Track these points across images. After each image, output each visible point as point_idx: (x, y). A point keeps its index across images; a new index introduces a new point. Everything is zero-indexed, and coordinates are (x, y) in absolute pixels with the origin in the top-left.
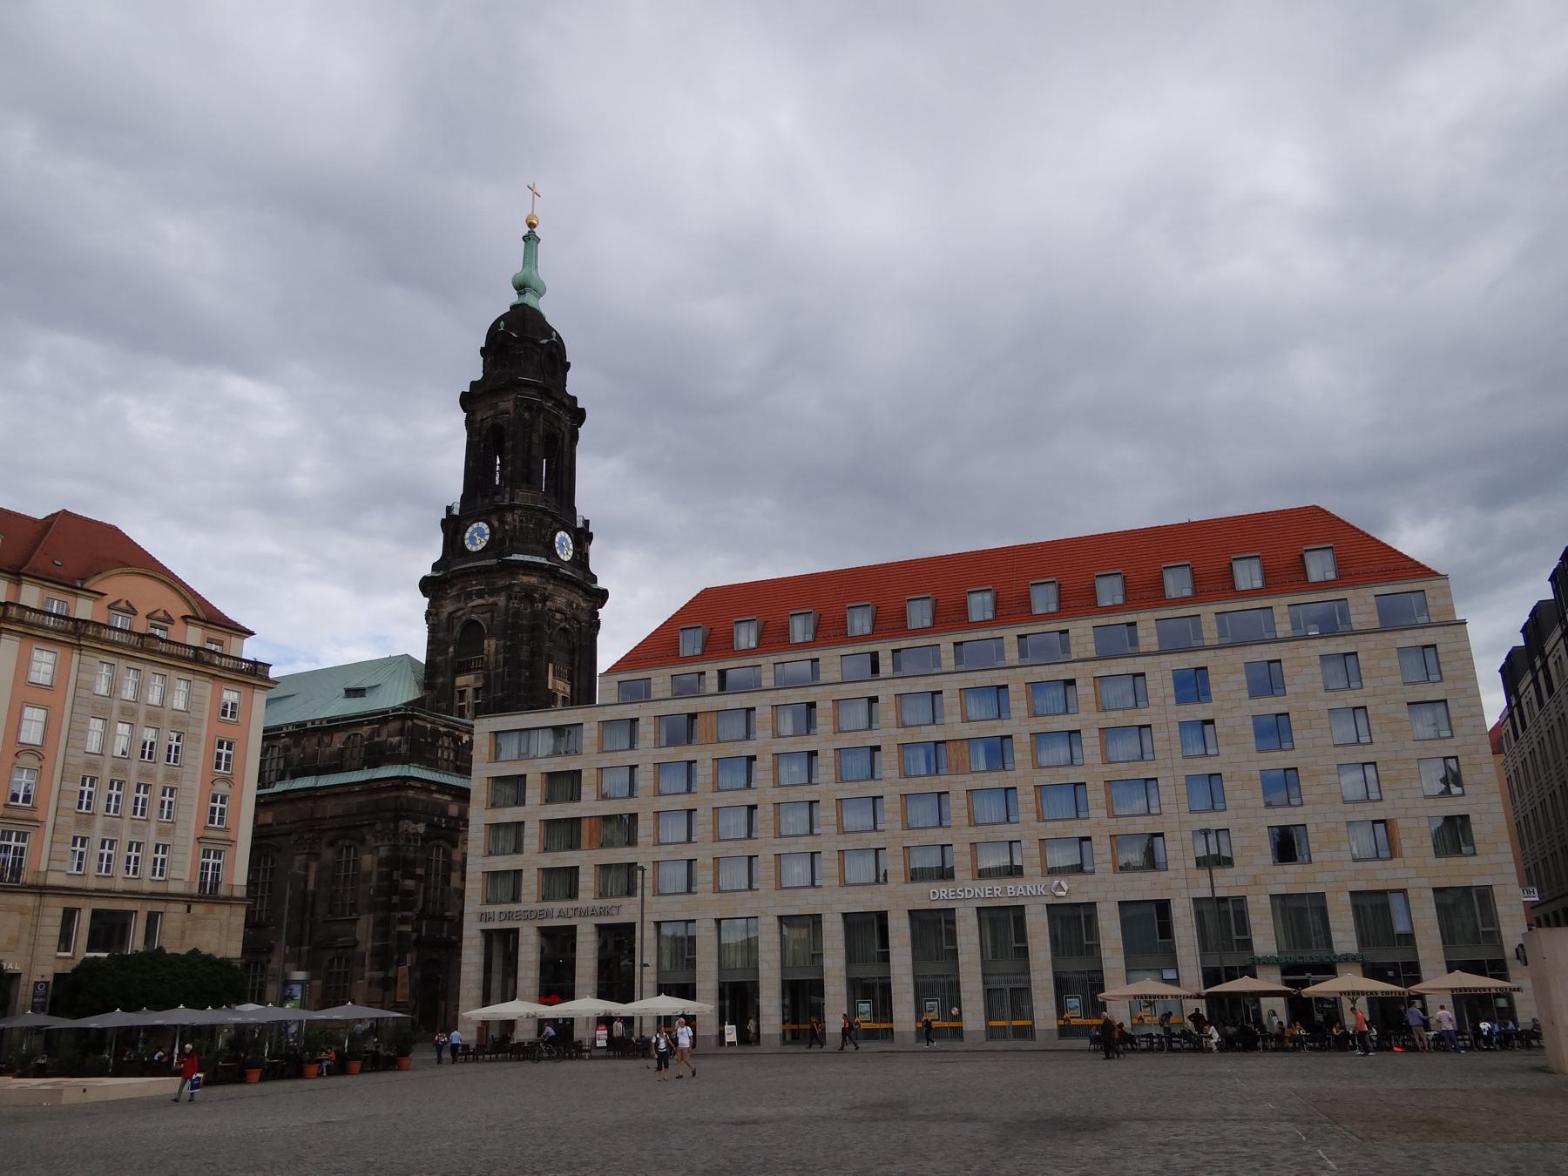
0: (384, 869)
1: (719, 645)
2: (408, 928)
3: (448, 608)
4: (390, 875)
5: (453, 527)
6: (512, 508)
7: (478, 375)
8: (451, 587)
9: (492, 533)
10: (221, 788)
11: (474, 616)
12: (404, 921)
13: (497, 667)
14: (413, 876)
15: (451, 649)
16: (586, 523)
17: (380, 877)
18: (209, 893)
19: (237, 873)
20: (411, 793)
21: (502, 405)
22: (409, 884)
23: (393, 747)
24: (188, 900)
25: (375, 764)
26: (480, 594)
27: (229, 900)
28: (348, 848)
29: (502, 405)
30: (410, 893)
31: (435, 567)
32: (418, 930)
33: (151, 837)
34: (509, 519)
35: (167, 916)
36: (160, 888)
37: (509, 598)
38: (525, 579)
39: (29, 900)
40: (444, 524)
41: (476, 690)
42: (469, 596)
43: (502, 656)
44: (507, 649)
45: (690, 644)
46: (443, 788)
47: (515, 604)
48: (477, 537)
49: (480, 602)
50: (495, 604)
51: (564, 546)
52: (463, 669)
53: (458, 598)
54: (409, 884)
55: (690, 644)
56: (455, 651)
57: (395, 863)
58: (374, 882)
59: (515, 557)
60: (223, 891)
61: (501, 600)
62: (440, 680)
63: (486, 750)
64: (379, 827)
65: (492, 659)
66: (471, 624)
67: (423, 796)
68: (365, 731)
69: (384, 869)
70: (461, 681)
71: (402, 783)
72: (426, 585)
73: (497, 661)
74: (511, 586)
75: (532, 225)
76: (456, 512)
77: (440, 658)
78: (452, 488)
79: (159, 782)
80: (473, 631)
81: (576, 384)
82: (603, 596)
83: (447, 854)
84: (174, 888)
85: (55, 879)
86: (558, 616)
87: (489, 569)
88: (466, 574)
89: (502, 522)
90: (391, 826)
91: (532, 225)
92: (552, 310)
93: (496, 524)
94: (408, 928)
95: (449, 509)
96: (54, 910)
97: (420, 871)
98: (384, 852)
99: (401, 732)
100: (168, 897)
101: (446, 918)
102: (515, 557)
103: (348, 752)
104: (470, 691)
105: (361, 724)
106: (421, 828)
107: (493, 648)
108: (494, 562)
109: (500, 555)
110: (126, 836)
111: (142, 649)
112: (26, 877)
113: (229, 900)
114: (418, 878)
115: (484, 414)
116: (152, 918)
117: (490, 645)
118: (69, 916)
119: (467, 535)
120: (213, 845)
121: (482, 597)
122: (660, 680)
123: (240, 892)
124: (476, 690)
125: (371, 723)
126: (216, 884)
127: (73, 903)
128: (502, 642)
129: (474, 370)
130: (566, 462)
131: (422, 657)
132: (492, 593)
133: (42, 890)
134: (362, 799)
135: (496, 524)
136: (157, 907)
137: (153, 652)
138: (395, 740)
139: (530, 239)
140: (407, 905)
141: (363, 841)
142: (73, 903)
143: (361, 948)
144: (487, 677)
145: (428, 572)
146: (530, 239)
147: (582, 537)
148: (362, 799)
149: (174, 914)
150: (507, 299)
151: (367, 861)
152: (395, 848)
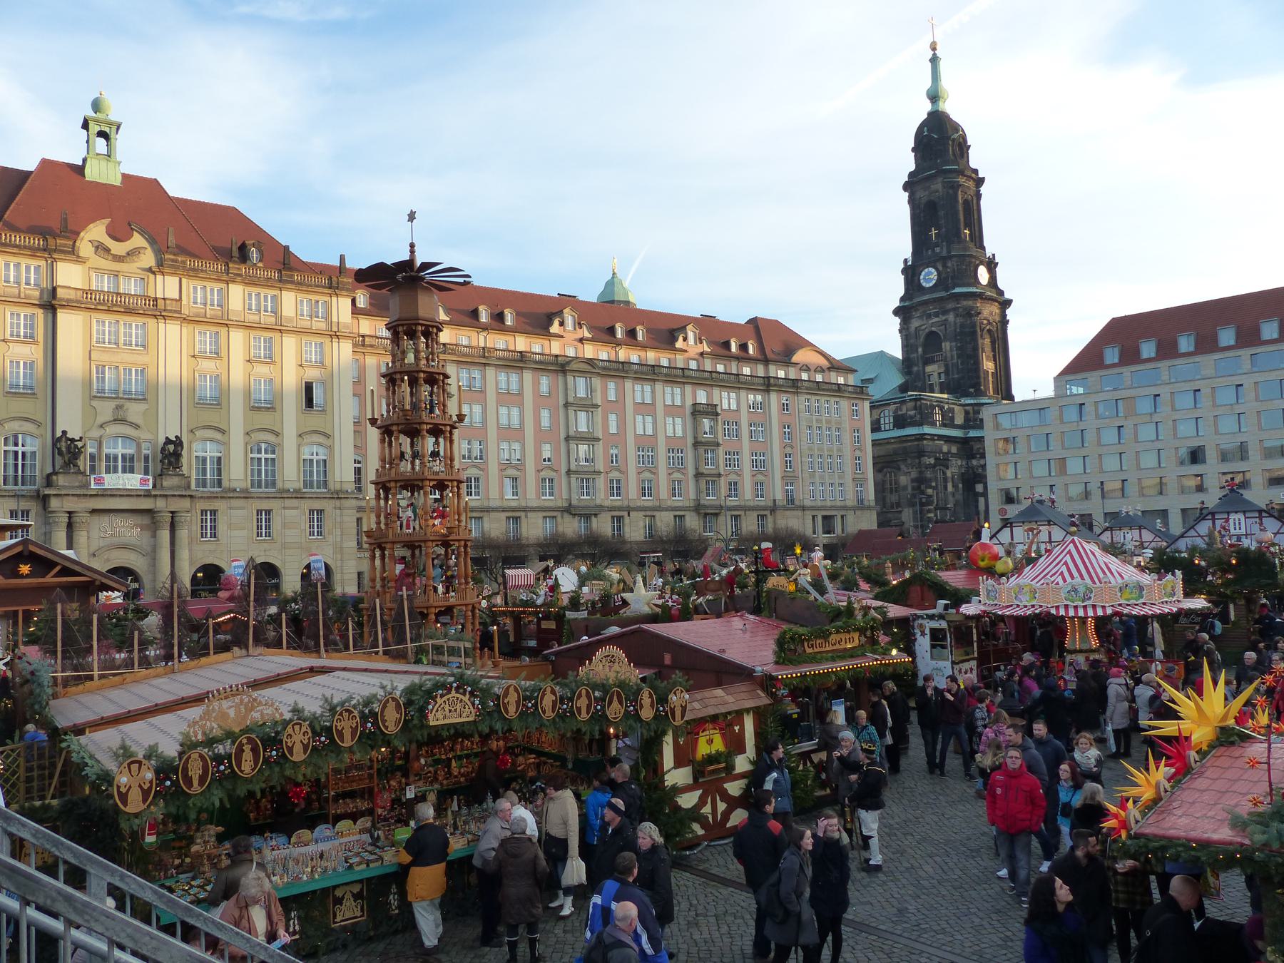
0: (915, 484)
1: (1130, 357)
2: (931, 515)
3: (915, 323)
4: (919, 488)
5: (911, 272)
6: (950, 257)
7: (912, 167)
8: (916, 311)
9: (939, 274)
10: (858, 453)
11: (933, 329)
12: (929, 511)
13: (952, 359)
14: (931, 487)
15: (920, 350)
16: (994, 255)
17: (913, 488)
18: (861, 506)
19: (870, 495)
20: (925, 442)
21: (934, 187)
22: (930, 491)
23: (911, 417)
24: (855, 509)
25: (903, 427)
26: (937, 315)
27: (869, 508)
28: (890, 473)
29: (934, 187)
30: (931, 496)
31: (902, 299)
32: (936, 515)
33: (837, 481)
34: (949, 264)
35: (848, 517)
36: (842, 504)
37: (957, 316)
38: (965, 303)
39: (800, 513)
40: (905, 271)
41: (939, 374)
42: (929, 316)
43: (955, 353)
44: (958, 348)
45: (1111, 355)
46: (940, 437)
47: (959, 320)
48: (929, 277)
49: (937, 319)
50: (946, 320)
51: (983, 275)
52: (928, 361)
53: (921, 317)
54: (930, 491)
55: (1111, 355)
56: (924, 351)
57: (920, 482)
58: (910, 489)
59: (957, 290)
60: (866, 503)
61: (951, 317)
62: (915, 369)
63: (991, 424)
64: (909, 461)
65: (949, 354)
66: (932, 333)
67: (931, 443)
68: (893, 407)
69: (915, 484)
70: (929, 369)
71: (921, 437)
72: (897, 312)
73: (952, 356)
74: (955, 309)
75: (934, 49)
76: (910, 263)
77: (915, 355)
78: (904, 248)
79: (835, 453)
80: (933, 340)
81: (976, 159)
82: (1008, 303)
83: (944, 473)
84: (850, 503)
85: (807, 503)
86: (985, 322)
87: (941, 299)
88: (926, 303)
89: (945, 266)
90: (917, 461)
91: (934, 49)
92: (953, 108)
93: (941, 268)
94: (931, 515)
95: (906, 261)
96: (809, 515)
97: (934, 484)
98: (914, 475)
99: (915, 408)
100: (845, 508)
101: (947, 509)
102: (957, 290)
103: (882, 419)
104: (936, 374)
105: (889, 404)
106: (932, 461)
107: (948, 348)
108: (943, 294)
109: (947, 289)
110: (828, 481)
111: (819, 390)
112: (797, 503)
113: (869, 508)
114: (935, 488)
115: (922, 194)
116: (842, 517)
117: (946, 346)
118: (814, 517)
119: (922, 277)
120: (859, 482)
121: (937, 316)
122: (1093, 379)
123: (873, 503)
124: (939, 374)
125: (895, 403)
126: (862, 501)
127: (815, 513)
128: (954, 344)
129: (908, 163)
130: (976, 217)
131: (897, 353)
132: (945, 312)
133: (803, 508)
134: (895, 446)
135: (941, 268)
136: (843, 513)
137: (823, 390)
138: (912, 413)
139: (934, 60)
140: (929, 503)
141: (899, 469)
142: (815, 513)
143: (906, 526)
144: (946, 366)
145: (897, 304)
146: (934, 60)
147: (992, 265)
148: (895, 446)
149: (850, 517)
150: (925, 108)
151: (904, 480)
152: (921, 472)
